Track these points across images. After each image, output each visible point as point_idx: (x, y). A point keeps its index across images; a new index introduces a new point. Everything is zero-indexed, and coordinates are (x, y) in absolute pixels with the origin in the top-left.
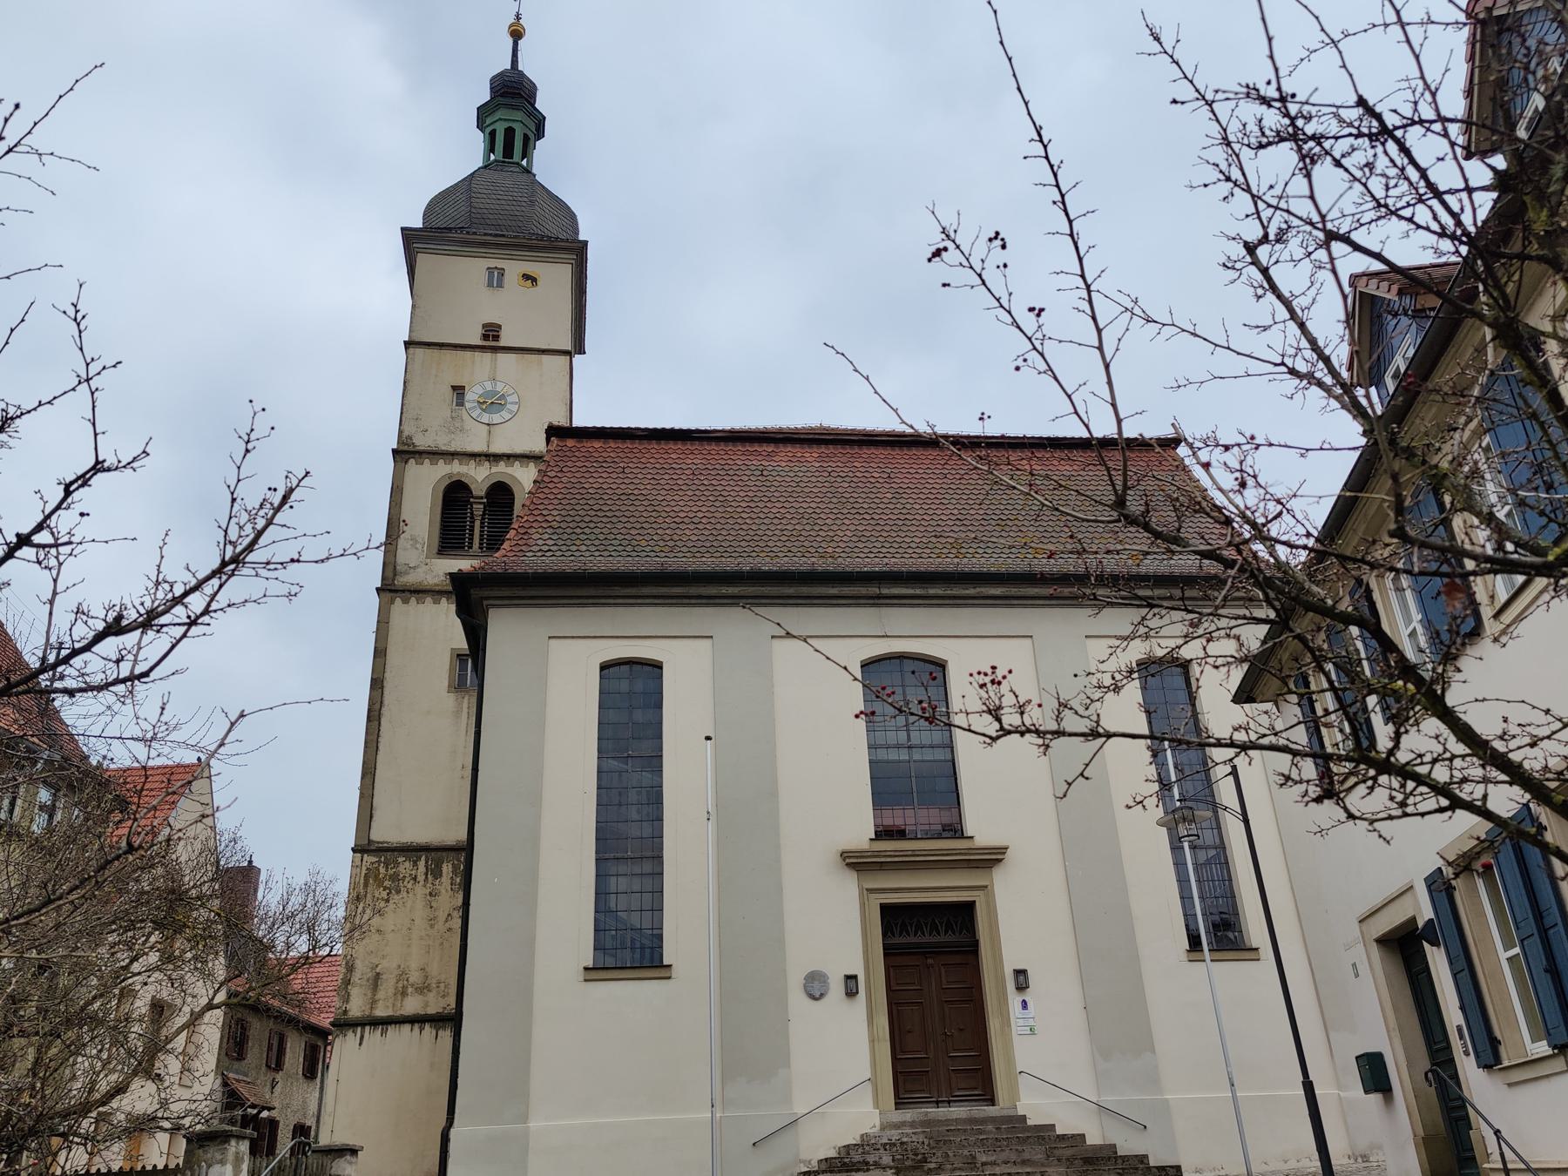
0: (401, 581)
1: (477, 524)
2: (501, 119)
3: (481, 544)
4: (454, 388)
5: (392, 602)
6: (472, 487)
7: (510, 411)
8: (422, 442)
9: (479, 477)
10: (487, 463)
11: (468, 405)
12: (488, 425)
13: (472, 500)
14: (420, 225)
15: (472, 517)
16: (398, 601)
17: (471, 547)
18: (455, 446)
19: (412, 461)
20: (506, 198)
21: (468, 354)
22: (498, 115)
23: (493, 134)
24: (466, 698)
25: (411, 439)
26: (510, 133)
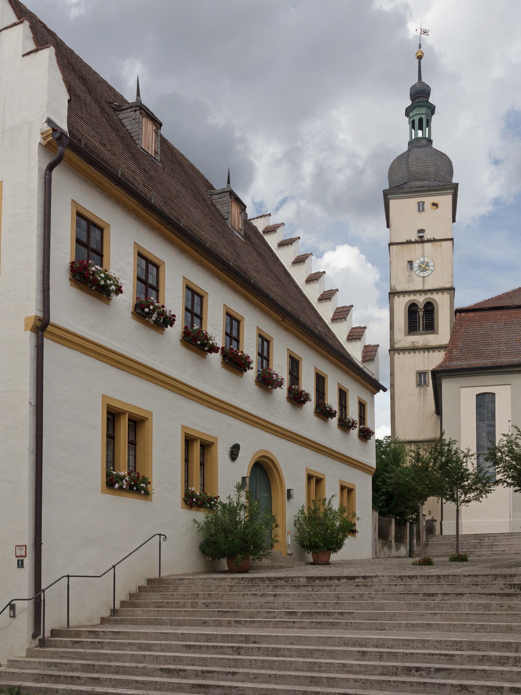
0: (397, 346)
1: (421, 320)
2: (416, 114)
3: (423, 328)
4: (409, 262)
5: (394, 354)
6: (419, 305)
7: (430, 270)
8: (399, 288)
9: (421, 299)
10: (423, 294)
11: (415, 269)
12: (423, 277)
13: (419, 310)
14: (388, 188)
15: (419, 317)
16: (396, 354)
17: (419, 330)
18: (411, 288)
19: (396, 296)
20: (423, 165)
21: (412, 246)
22: (415, 112)
23: (413, 122)
24: (423, 389)
25: (395, 287)
26: (421, 120)
